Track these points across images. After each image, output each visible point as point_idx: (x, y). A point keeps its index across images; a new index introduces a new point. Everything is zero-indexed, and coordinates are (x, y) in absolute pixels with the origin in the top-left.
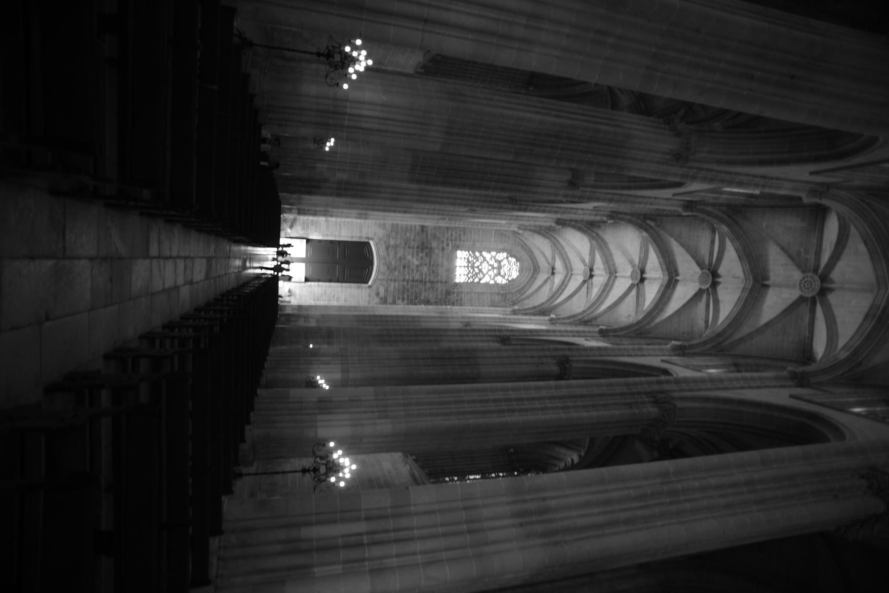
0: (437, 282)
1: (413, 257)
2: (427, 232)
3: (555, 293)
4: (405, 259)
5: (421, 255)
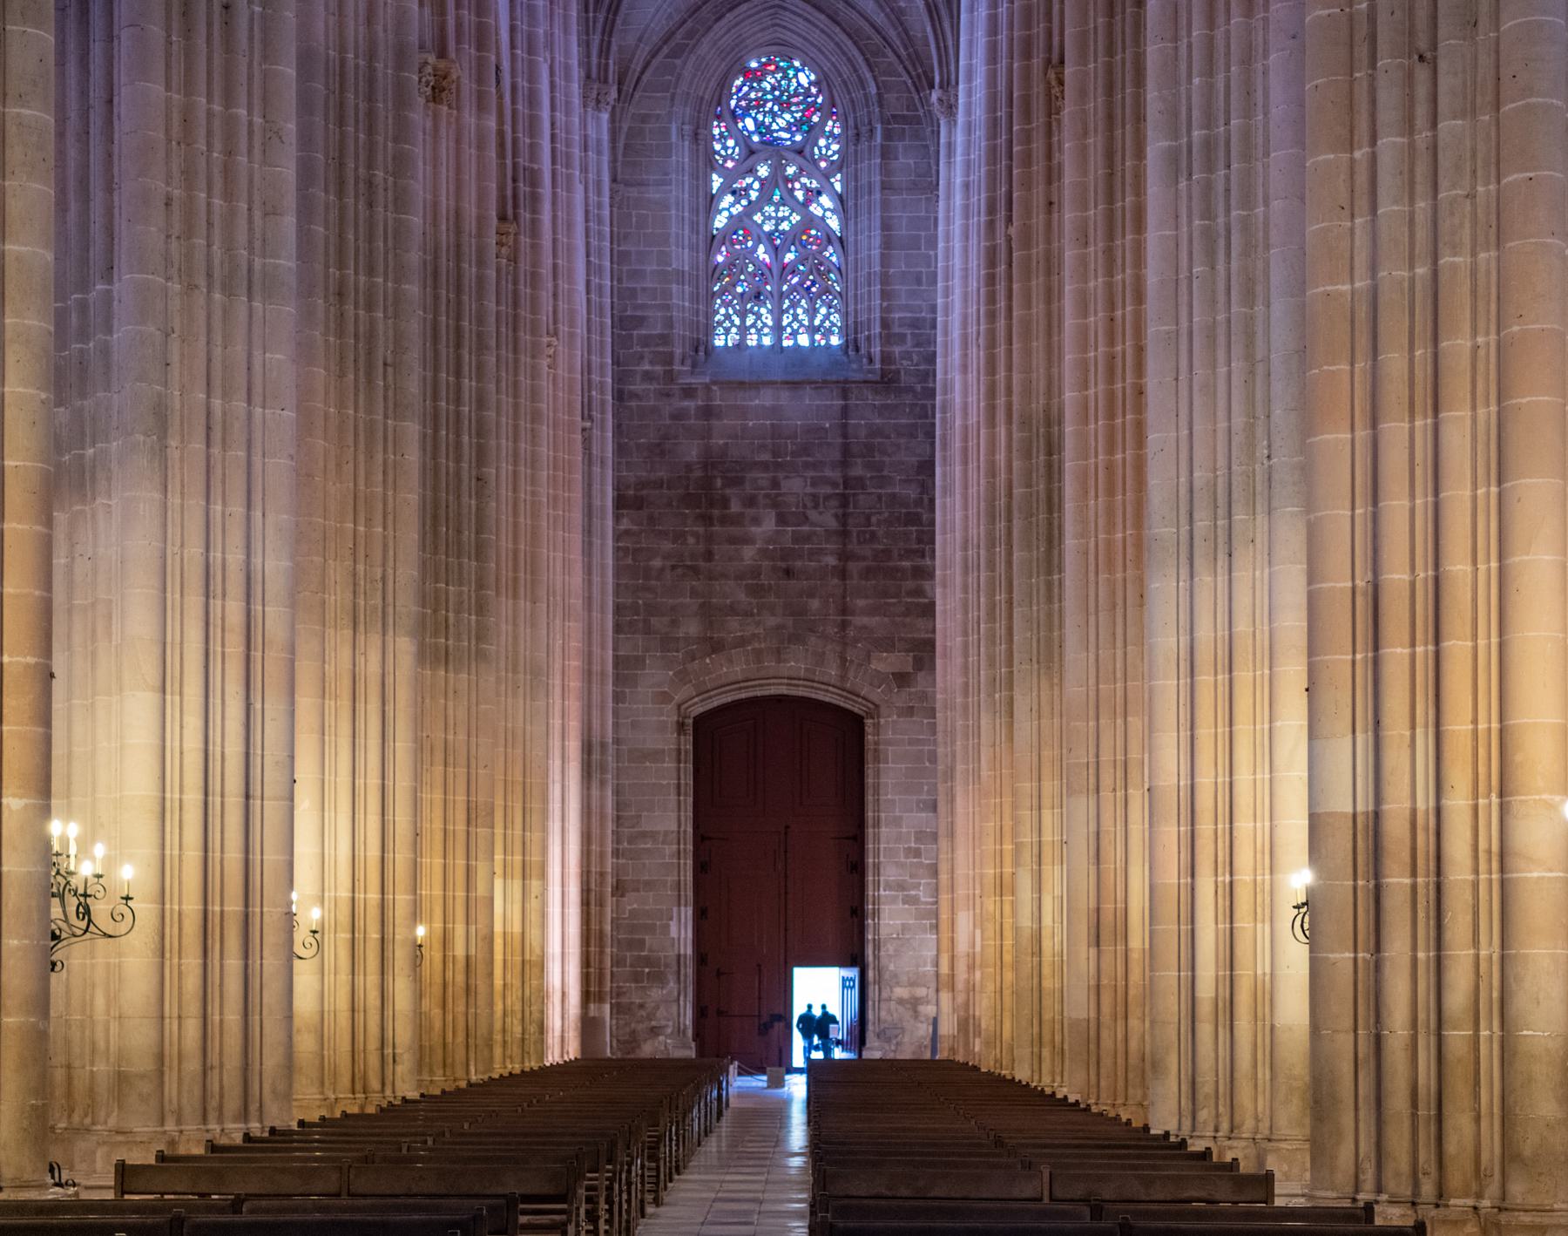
0: (844, 432)
1: (747, 540)
2: (642, 484)
4: (755, 572)
5: (735, 507)
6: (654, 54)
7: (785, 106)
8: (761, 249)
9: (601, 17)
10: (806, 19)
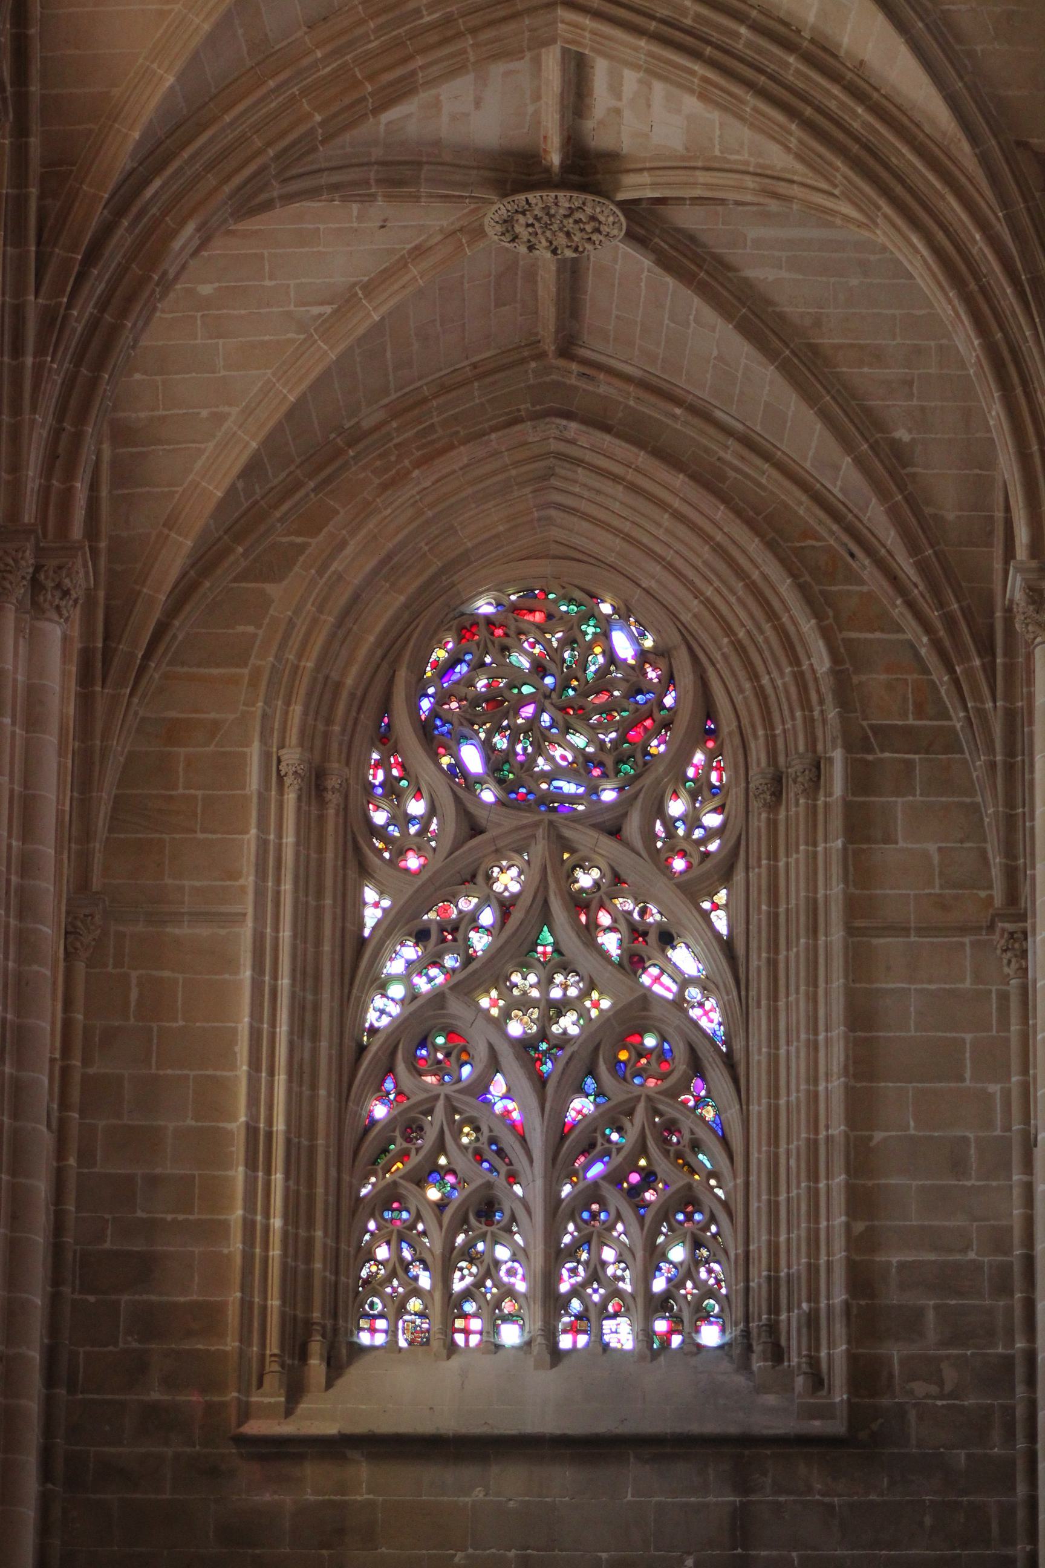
3: (822, 129)
6: (206, 561)
7: (573, 714)
8: (499, 1085)
9: (58, 369)
10: (634, 488)
